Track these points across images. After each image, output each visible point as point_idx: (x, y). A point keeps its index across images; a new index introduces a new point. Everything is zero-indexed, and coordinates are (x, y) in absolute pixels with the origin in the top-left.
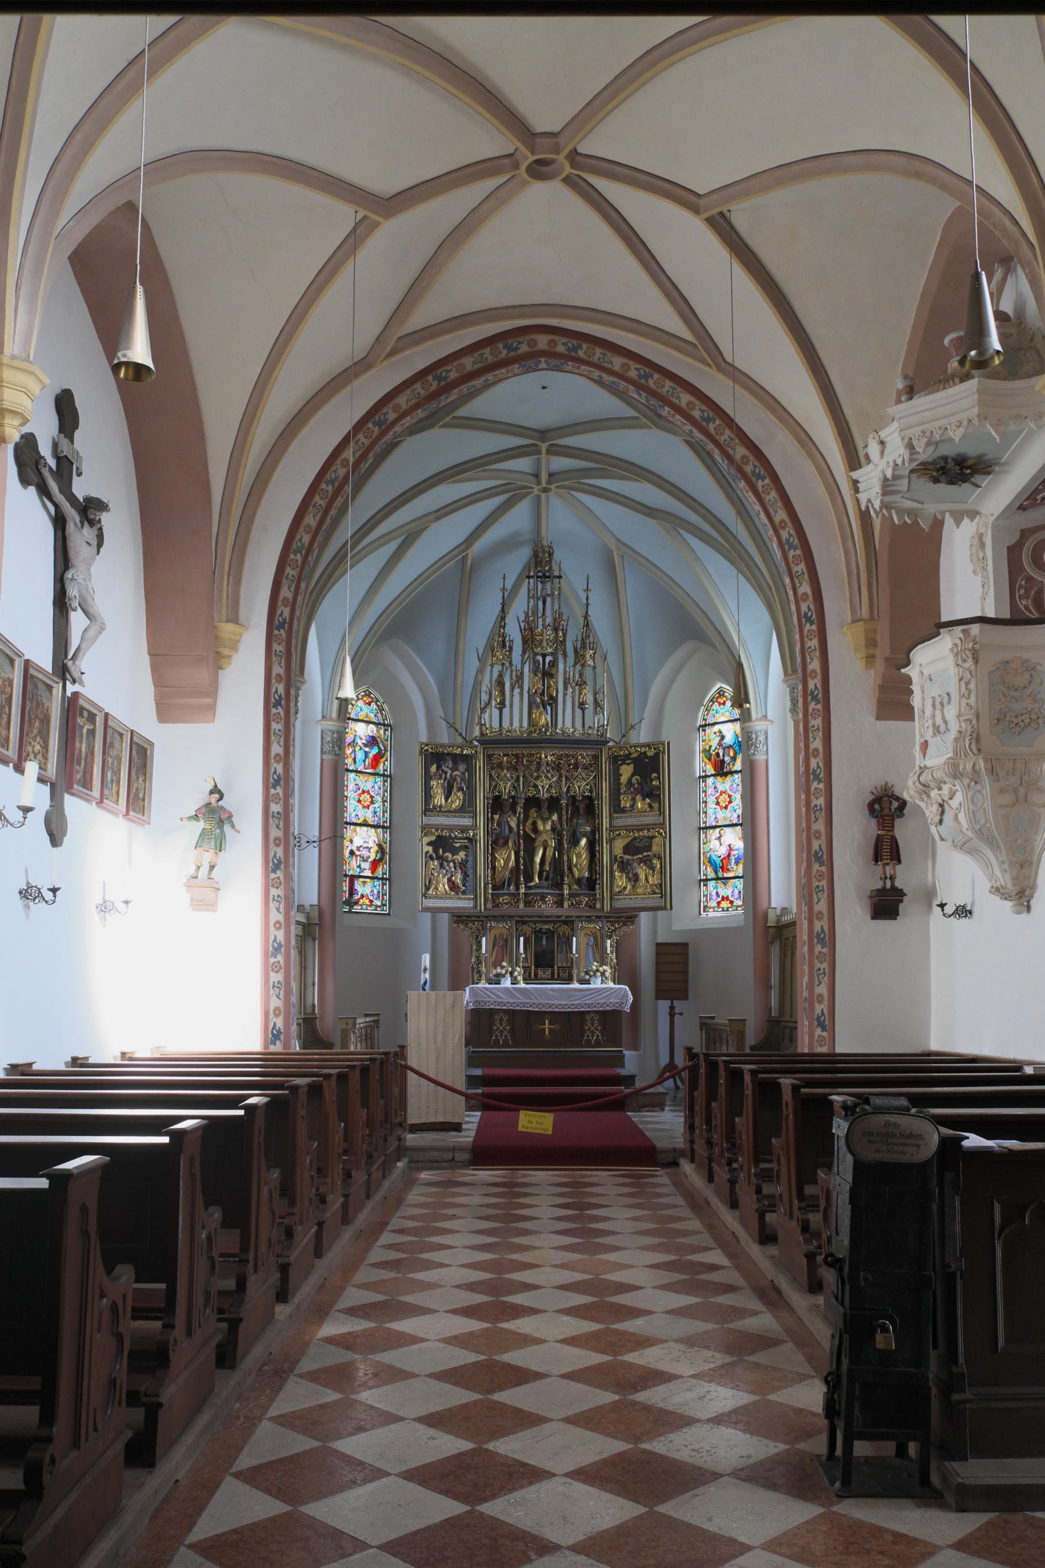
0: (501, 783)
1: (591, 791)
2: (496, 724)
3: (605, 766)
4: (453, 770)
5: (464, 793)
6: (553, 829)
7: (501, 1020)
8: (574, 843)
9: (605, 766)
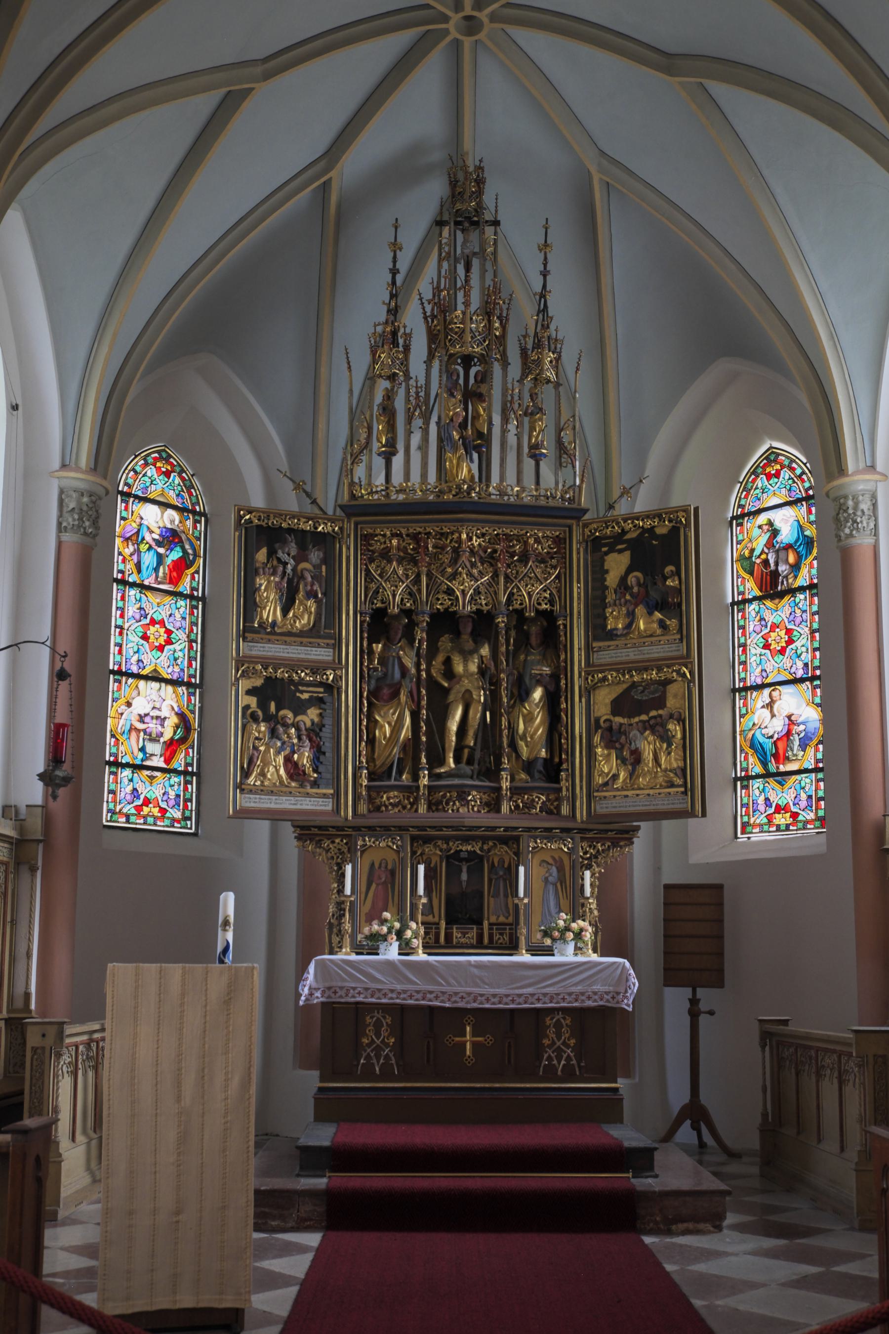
0: (387, 585)
1: (551, 602)
2: (379, 480)
3: (578, 555)
4: (298, 559)
5: (318, 602)
6: (482, 672)
7: (378, 1025)
8: (520, 695)
9: (578, 555)
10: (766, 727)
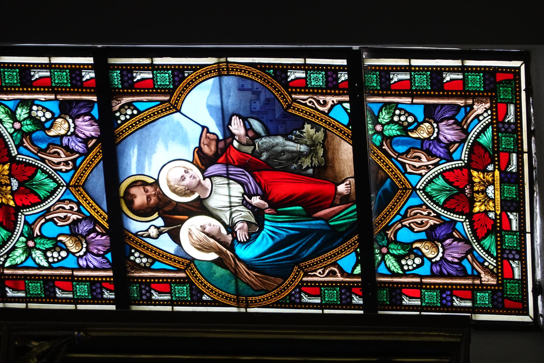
10: (231, 228)
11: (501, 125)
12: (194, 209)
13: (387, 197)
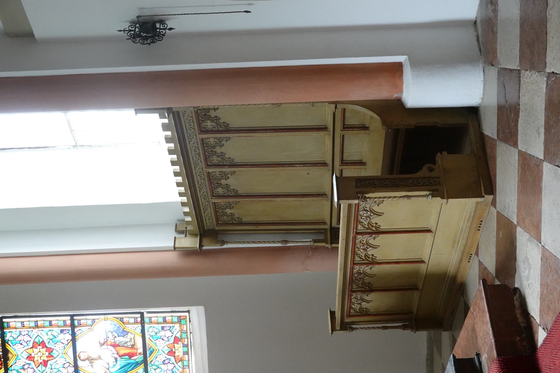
11: (182, 331)
12: (97, 358)
13: (151, 353)
